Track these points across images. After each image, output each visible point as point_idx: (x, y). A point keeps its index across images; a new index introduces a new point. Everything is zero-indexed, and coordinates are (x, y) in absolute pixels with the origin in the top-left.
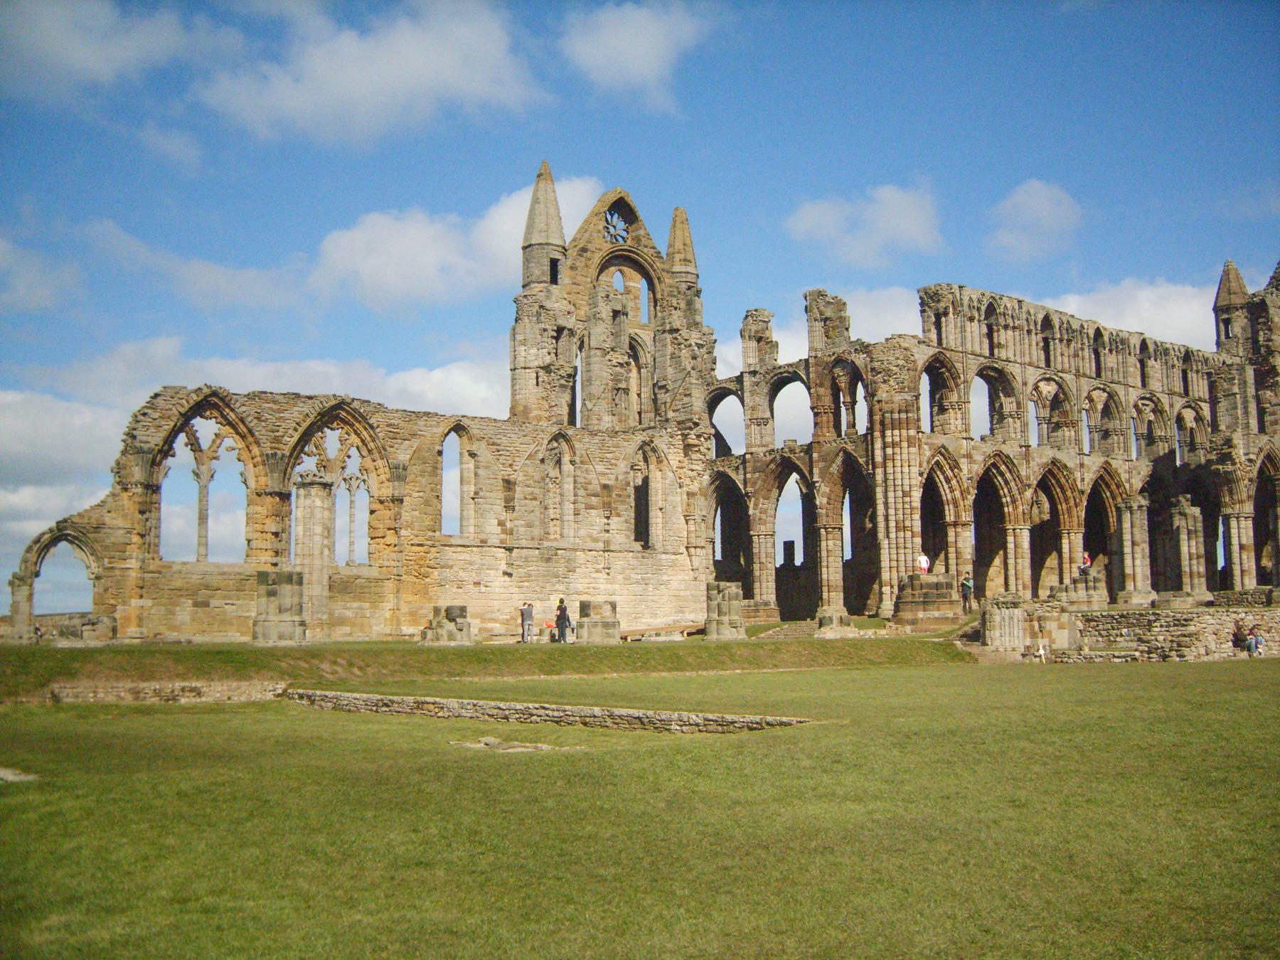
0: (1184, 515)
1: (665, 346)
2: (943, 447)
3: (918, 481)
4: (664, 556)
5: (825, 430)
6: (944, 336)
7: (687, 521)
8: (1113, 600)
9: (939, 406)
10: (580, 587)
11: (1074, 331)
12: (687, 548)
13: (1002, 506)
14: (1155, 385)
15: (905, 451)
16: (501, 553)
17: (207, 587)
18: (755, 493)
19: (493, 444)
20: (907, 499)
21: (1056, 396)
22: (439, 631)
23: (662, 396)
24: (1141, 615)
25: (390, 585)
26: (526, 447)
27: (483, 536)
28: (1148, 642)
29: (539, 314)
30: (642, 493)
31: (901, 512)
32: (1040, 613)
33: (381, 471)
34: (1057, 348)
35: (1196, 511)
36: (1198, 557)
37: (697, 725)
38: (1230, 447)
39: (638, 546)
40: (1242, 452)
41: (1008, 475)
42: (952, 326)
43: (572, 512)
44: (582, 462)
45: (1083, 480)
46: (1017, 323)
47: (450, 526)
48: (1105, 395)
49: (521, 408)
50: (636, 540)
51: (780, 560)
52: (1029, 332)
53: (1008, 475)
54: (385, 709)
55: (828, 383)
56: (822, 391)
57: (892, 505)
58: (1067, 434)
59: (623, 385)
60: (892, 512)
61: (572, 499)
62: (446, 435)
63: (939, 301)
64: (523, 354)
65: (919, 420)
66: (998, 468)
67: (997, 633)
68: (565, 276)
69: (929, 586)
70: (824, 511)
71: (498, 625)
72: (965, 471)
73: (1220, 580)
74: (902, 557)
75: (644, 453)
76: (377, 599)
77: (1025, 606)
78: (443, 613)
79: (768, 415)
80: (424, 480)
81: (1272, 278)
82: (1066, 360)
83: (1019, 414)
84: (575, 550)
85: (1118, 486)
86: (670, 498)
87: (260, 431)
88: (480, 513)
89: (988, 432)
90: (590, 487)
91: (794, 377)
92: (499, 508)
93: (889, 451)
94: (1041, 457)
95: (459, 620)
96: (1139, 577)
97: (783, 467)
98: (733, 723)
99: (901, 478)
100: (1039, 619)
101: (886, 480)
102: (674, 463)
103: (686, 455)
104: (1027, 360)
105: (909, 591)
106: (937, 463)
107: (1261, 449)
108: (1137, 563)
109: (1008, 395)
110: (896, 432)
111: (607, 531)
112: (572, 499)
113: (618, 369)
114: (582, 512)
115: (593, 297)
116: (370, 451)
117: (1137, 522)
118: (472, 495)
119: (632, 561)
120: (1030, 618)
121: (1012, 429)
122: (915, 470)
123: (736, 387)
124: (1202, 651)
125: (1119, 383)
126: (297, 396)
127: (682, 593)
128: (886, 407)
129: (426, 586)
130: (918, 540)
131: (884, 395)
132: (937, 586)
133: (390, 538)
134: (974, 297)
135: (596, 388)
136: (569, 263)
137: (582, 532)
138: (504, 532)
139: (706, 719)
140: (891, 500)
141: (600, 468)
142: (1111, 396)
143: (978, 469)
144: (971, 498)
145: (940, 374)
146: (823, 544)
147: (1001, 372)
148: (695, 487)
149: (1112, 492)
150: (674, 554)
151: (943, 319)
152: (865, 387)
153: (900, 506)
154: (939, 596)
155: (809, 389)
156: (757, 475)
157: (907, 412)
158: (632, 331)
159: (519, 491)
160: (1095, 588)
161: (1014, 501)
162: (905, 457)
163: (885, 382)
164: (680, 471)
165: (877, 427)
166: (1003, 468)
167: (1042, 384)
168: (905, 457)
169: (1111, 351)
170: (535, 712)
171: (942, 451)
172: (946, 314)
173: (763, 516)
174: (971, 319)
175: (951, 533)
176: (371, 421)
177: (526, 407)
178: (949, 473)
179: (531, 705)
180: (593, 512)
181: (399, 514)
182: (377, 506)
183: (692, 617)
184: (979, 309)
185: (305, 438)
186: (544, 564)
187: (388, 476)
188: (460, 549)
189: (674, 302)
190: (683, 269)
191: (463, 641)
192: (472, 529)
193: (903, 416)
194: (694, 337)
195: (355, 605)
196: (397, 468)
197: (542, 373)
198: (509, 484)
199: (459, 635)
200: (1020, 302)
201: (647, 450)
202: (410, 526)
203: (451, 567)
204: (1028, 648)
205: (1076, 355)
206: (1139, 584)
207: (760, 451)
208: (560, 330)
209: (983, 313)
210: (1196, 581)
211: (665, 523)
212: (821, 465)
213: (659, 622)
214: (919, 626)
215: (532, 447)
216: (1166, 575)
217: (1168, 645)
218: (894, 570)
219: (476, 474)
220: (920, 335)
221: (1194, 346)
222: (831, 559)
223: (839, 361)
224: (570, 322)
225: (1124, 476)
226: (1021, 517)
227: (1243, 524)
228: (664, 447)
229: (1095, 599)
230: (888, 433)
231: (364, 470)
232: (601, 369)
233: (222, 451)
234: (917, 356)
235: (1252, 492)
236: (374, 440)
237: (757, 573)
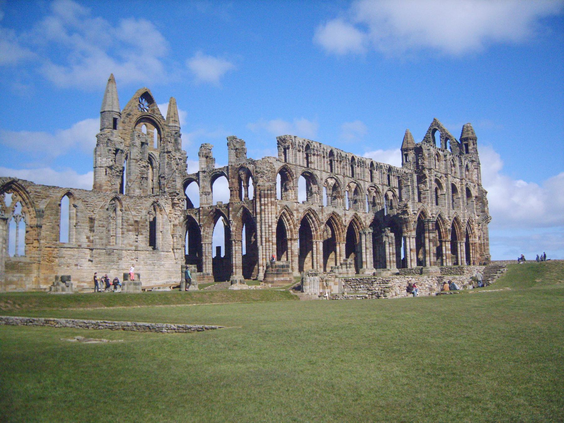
0: (388, 236)
1: (164, 159)
2: (286, 206)
3: (275, 220)
4: (162, 253)
5: (235, 197)
6: (287, 158)
7: (173, 237)
8: (358, 272)
9: (285, 188)
10: (124, 267)
11: (343, 157)
12: (173, 249)
13: (311, 232)
14: (376, 181)
15: (270, 207)
16: (88, 251)
18: (204, 225)
19: (85, 201)
20: (270, 228)
21: (335, 184)
22: (58, 287)
23: (163, 181)
24: (369, 279)
25: (35, 266)
26: (101, 202)
27: (79, 244)
28: (372, 290)
29: (107, 143)
30: (153, 225)
31: (267, 234)
32: (326, 278)
33: (32, 213)
34: (335, 164)
35: (392, 235)
36: (393, 254)
37: (174, 329)
38: (407, 208)
39: (150, 248)
40: (411, 210)
41: (314, 219)
42: (291, 153)
43: (121, 233)
44: (126, 210)
45: (345, 221)
46: (319, 153)
47: (64, 238)
48: (356, 185)
49: (98, 185)
50: (150, 245)
51: (214, 255)
52: (324, 157)
54: (30, 324)
55: (237, 177)
56: (234, 180)
57: (264, 231)
58: (339, 201)
59: (145, 176)
60: (263, 234)
61: (121, 227)
62: (63, 197)
63: (285, 143)
64: (100, 160)
65: (276, 194)
66: (309, 215)
67: (308, 287)
68: (120, 126)
69: (279, 266)
70: (234, 233)
71: (86, 284)
72: (295, 217)
73: (402, 264)
74: (268, 254)
75: (154, 207)
76: (29, 272)
77: (320, 275)
78: (60, 279)
79: (210, 190)
80: (52, 218)
81: (425, 137)
82: (339, 169)
83: (319, 192)
84: (122, 250)
85: (360, 224)
86: (165, 227)
88: (78, 233)
89: (306, 200)
90: (129, 222)
91: (222, 174)
92: (87, 230)
93: (263, 207)
94: (328, 211)
95: (67, 282)
96: (368, 263)
97: (216, 213)
98: (190, 328)
99: (268, 220)
100: (326, 281)
101: (261, 220)
102: (168, 211)
103: (173, 208)
104: (323, 169)
105: (270, 268)
106: (284, 213)
107: (419, 209)
108: (368, 257)
109: (314, 184)
110: (266, 199)
111: (137, 242)
112: (121, 227)
113: (143, 168)
114: (125, 233)
115: (132, 135)
116: (26, 204)
117: (368, 239)
118: (74, 224)
119: (148, 255)
120: (322, 280)
121: (316, 199)
122: (274, 216)
123: (196, 178)
124: (394, 294)
125: (361, 180)
127: (170, 269)
128: (262, 188)
129: (52, 266)
130: (275, 246)
131: (261, 183)
132: (283, 266)
133: (36, 244)
134: (301, 141)
135: (133, 177)
136: (122, 120)
137: (125, 242)
138: (89, 241)
139: (178, 327)
140: (263, 229)
141: (134, 213)
142: (358, 185)
143: (301, 216)
144: (298, 228)
145: (285, 174)
146: (234, 248)
147: (311, 174)
148: (177, 222)
149: (358, 227)
150: (167, 252)
151: (287, 150)
152: (253, 179)
153: (267, 231)
154: (283, 271)
155: (228, 179)
156: (205, 217)
157: (271, 190)
158: (150, 152)
159: (96, 223)
160: (350, 267)
161: (316, 230)
162: (270, 210)
163: (261, 177)
164: (170, 215)
165: (258, 197)
166: (312, 215)
167: (329, 180)
168: (270, 210)
169: (358, 166)
170: (101, 324)
171: (286, 208)
172: (288, 148)
173: (207, 235)
174: (299, 151)
175: (289, 243)
176: (28, 190)
177: (100, 185)
178: (289, 217)
179: (99, 321)
180: (130, 233)
181: (40, 233)
182: (29, 229)
183: (175, 280)
184: (302, 147)
186: (107, 256)
187: (35, 215)
188: (68, 249)
189: (169, 139)
190: (174, 125)
191: (68, 291)
192: (74, 240)
193: (269, 192)
194: (178, 155)
195: (18, 275)
196: (39, 211)
197: (108, 169)
198: (92, 220)
199: (67, 289)
200: (320, 144)
201: (155, 205)
202: (45, 238)
203: (64, 257)
204: (321, 293)
205: (343, 168)
206: (368, 265)
207: (206, 206)
208: (117, 150)
209: (304, 148)
210: (392, 264)
211: (163, 238)
212: (233, 213)
213: (160, 282)
214: (275, 284)
215: (103, 203)
216: (380, 262)
217: (380, 291)
218: (264, 260)
219: (77, 215)
220: (277, 157)
221: (392, 165)
222: (237, 254)
223: (242, 168)
224: (121, 147)
225: (363, 220)
226: (319, 236)
227: (411, 239)
228: (163, 204)
229: (350, 272)
230: (263, 199)
231: (23, 212)
232: (135, 168)
234: (275, 166)
235: (415, 227)
236: (28, 199)
237: (204, 261)
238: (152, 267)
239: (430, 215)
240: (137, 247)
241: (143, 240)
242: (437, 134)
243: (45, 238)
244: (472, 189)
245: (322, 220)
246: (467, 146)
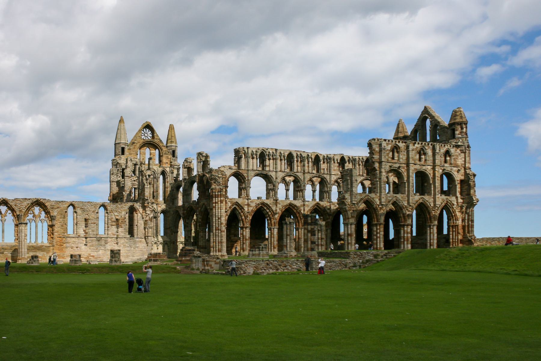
16: (84, 239)
17: (3, 249)
39: (129, 236)
46: (274, 157)
47: (70, 231)
53: (268, 211)
86: (139, 222)
87: (16, 209)
111: (117, 232)
126: (26, 199)
134: (254, 151)
141: (116, 214)
159: (90, 221)
184: (256, 155)
185: (28, 209)
198: (86, 220)
200: (276, 150)
233: (8, 214)
238: (129, 249)
239: (378, 203)
240: (117, 235)
241: (123, 231)
242: (428, 122)
243: (57, 232)
244: (456, 173)
245: (276, 210)
246: (454, 131)
